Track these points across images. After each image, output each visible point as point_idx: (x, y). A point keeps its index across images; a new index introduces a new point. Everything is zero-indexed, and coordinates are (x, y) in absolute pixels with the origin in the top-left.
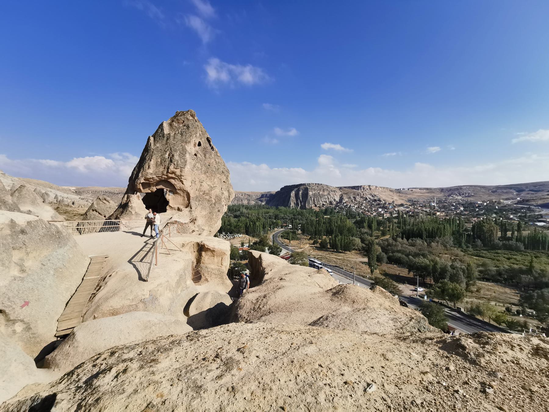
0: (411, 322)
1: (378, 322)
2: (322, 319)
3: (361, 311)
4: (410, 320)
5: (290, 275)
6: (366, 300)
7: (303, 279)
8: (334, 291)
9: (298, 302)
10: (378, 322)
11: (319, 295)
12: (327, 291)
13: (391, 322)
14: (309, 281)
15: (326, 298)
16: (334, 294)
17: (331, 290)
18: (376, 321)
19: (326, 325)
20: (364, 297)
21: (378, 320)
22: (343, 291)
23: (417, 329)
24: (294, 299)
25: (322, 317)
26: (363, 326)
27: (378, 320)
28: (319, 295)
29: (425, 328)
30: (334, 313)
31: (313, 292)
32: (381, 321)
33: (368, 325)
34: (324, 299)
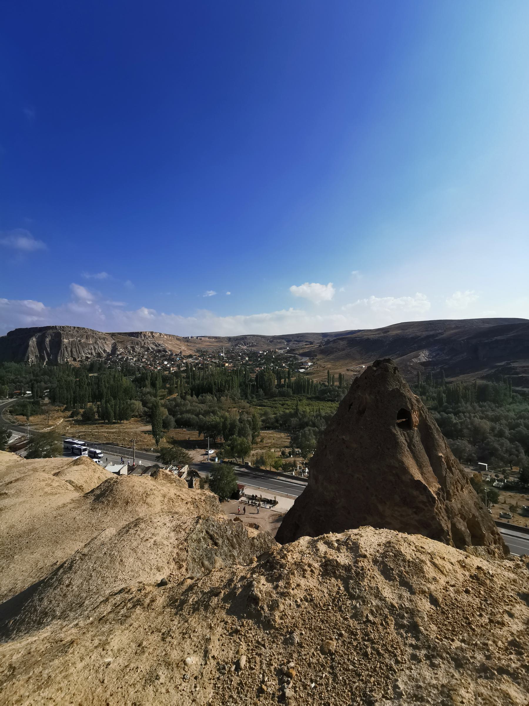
0: (198, 526)
1: (155, 543)
2: (61, 571)
3: (132, 531)
4: (197, 522)
5: (19, 483)
6: (144, 495)
7: (43, 484)
8: (98, 492)
9: (31, 531)
10: (155, 543)
11: (72, 505)
12: (86, 496)
13: (172, 534)
14: (55, 484)
15: (84, 508)
16: (98, 498)
17: (93, 491)
18: (152, 541)
19: (67, 582)
20: (141, 490)
21: (155, 538)
22: (112, 490)
23: (204, 532)
24: (21, 527)
25: (62, 566)
26: (131, 560)
27: (155, 538)
28: (72, 505)
29: (213, 526)
30: (86, 551)
31: (60, 504)
32: (158, 539)
33: (140, 554)
34: (79, 511)
